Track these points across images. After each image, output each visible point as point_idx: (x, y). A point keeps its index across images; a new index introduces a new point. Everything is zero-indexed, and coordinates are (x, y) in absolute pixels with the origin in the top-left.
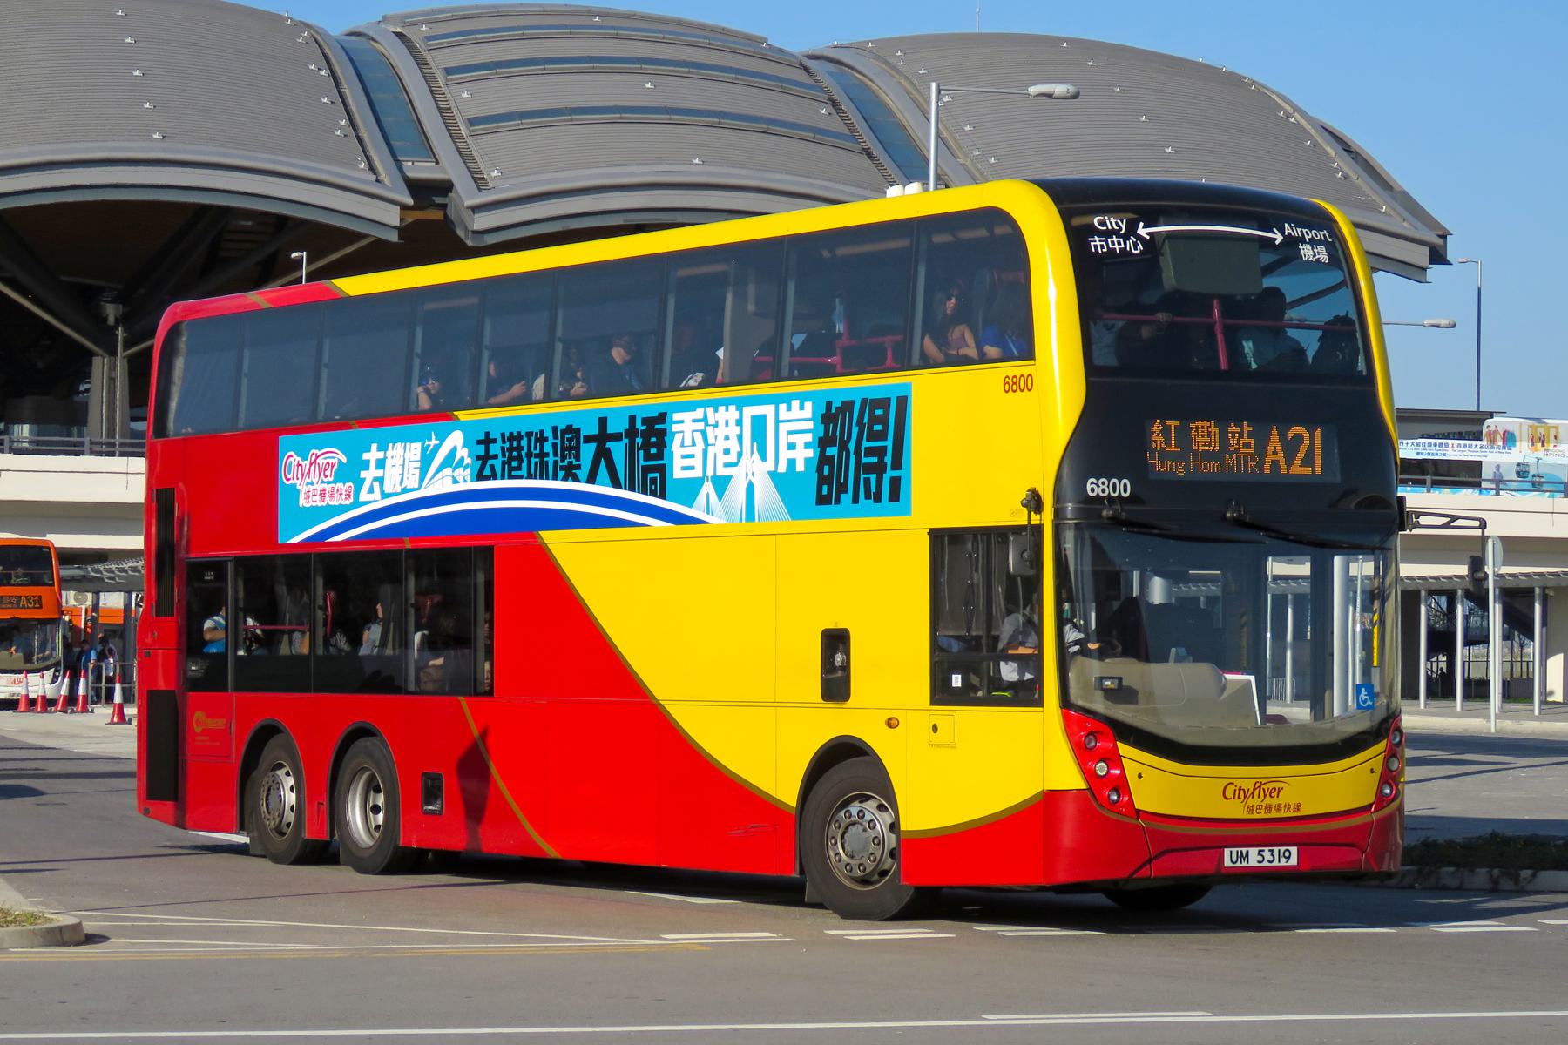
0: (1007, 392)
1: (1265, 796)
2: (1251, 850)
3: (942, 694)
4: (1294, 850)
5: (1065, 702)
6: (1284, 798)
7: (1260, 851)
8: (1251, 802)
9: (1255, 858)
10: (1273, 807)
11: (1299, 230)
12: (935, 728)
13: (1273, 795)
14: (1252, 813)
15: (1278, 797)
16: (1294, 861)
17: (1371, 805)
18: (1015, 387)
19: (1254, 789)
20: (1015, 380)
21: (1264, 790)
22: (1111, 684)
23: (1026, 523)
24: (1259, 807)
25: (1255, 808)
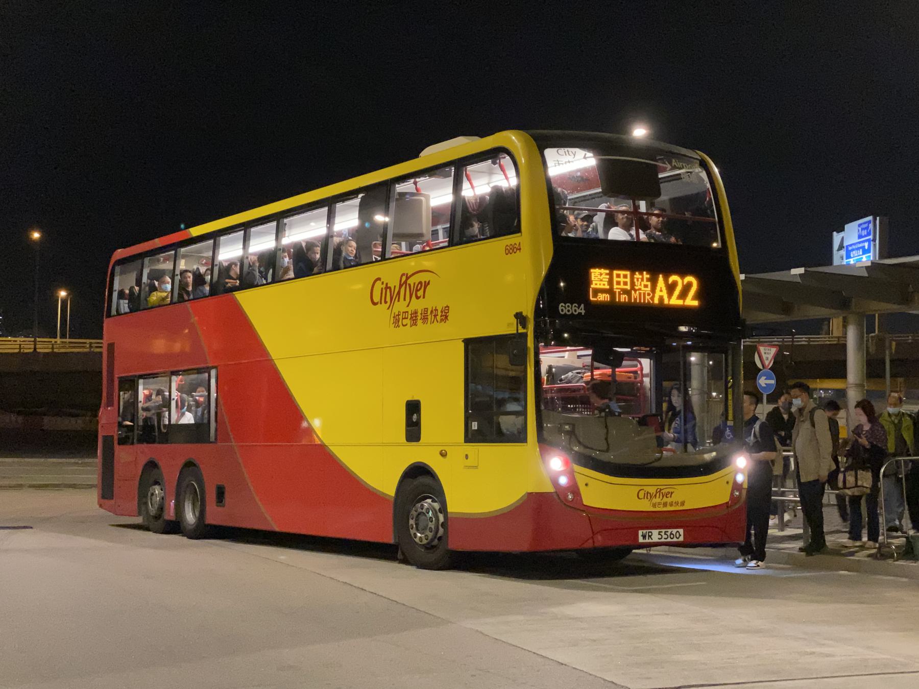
0: (507, 254)
1: (663, 497)
2: (653, 531)
3: (471, 437)
4: (681, 531)
5: (541, 439)
6: (674, 498)
7: (659, 532)
8: (654, 500)
9: (656, 536)
10: (668, 504)
11: (681, 164)
12: (467, 457)
13: (668, 496)
14: (655, 507)
15: (671, 497)
16: (681, 539)
17: (727, 503)
18: (511, 250)
19: (657, 493)
20: (511, 247)
21: (662, 493)
22: (569, 427)
23: (515, 332)
24: (659, 504)
25: (657, 504)
